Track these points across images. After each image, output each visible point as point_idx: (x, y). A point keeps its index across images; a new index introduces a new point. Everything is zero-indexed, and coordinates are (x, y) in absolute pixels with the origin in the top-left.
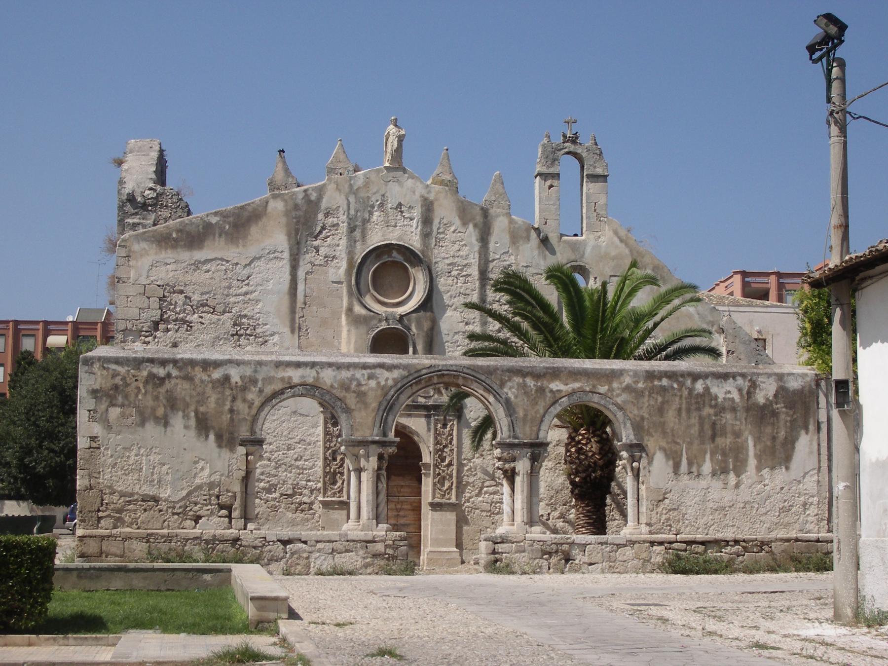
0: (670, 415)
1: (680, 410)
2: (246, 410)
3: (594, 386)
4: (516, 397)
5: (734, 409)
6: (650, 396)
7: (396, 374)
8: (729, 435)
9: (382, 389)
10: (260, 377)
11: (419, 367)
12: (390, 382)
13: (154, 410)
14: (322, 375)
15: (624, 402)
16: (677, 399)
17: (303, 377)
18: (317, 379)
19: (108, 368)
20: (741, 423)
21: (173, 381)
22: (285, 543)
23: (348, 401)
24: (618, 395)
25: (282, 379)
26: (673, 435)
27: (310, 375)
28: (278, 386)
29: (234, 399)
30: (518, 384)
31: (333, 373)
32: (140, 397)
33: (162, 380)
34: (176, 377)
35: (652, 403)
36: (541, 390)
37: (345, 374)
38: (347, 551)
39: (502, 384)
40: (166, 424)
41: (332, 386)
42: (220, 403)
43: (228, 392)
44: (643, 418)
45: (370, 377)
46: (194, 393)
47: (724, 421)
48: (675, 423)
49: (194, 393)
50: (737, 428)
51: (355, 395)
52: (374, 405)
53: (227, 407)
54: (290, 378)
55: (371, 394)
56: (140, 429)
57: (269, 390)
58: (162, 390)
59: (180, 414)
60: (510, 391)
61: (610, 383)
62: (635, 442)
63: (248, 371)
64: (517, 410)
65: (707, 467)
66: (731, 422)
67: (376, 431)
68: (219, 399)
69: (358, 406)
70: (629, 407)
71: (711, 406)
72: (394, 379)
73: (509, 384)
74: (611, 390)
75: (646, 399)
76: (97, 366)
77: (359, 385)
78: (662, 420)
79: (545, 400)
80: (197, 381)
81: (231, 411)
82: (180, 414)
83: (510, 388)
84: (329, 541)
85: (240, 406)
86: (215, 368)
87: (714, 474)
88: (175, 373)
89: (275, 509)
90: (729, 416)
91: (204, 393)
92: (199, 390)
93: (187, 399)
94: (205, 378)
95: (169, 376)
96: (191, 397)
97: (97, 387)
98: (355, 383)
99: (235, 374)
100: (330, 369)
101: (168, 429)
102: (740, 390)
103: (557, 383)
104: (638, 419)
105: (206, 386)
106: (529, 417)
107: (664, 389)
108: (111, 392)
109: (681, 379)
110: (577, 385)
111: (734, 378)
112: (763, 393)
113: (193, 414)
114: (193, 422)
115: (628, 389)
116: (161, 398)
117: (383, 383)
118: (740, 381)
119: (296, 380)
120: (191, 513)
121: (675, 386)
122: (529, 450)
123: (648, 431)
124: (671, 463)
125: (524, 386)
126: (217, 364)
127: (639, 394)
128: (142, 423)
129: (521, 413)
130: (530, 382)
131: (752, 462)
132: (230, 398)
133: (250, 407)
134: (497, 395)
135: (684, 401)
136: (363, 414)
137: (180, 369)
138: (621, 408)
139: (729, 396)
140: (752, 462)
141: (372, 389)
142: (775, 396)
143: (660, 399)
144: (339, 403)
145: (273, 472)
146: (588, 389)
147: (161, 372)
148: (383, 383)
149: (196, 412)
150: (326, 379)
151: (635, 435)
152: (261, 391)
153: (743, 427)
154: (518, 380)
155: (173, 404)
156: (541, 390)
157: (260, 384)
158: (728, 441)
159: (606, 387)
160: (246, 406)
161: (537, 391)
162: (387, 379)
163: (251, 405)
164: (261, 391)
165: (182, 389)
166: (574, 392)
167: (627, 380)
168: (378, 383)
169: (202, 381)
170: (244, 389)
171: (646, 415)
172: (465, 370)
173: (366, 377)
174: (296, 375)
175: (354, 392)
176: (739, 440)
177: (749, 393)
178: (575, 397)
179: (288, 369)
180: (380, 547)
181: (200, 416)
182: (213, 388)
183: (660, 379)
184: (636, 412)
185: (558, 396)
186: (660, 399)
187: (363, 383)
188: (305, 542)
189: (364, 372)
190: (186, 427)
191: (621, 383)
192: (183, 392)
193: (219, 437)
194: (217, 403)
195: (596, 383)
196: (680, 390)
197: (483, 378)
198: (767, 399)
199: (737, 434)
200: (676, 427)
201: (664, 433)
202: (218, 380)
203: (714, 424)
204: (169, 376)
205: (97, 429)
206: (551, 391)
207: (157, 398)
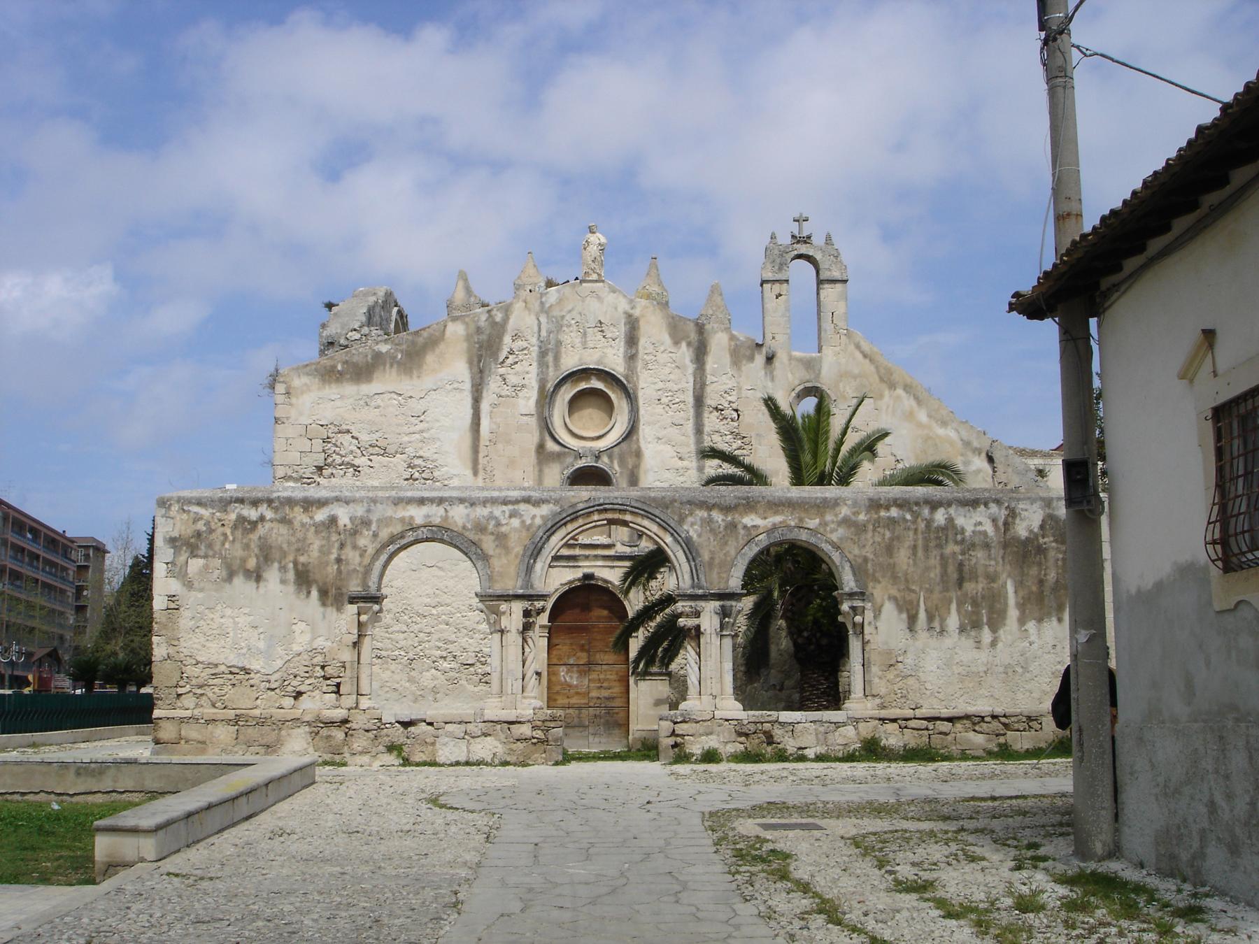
0: (902, 557)
1: (915, 547)
2: (357, 559)
3: (801, 520)
4: (699, 536)
5: (987, 546)
6: (874, 530)
7: (545, 510)
8: (980, 579)
9: (528, 530)
10: (374, 517)
11: (574, 501)
12: (538, 521)
13: (244, 560)
14: (451, 514)
15: (841, 539)
16: (911, 533)
17: (428, 516)
18: (446, 518)
19: (189, 511)
20: (997, 563)
21: (268, 525)
22: (406, 724)
23: (485, 546)
24: (832, 531)
25: (402, 520)
26: (907, 581)
27: (436, 513)
28: (397, 529)
29: (342, 546)
30: (702, 519)
31: (466, 511)
32: (227, 545)
33: (254, 524)
34: (271, 521)
35: (878, 539)
36: (732, 526)
37: (481, 512)
38: (486, 735)
39: (682, 520)
40: (259, 578)
41: (464, 527)
42: (324, 552)
43: (334, 537)
44: (866, 560)
45: (513, 515)
46: (293, 540)
47: (974, 561)
48: (908, 565)
49: (293, 540)
50: (991, 569)
51: (492, 537)
52: (519, 550)
53: (333, 556)
54: (412, 518)
55: (514, 537)
56: (227, 585)
57: (385, 534)
58: (254, 537)
59: (276, 565)
60: (692, 529)
61: (822, 515)
62: (856, 590)
63: (360, 511)
64: (701, 551)
65: (953, 621)
66: (983, 562)
67: (519, 583)
68: (322, 546)
69: (498, 551)
70: (848, 546)
71: (956, 542)
72: (542, 517)
73: (690, 519)
74: (824, 524)
75: (870, 534)
76: (175, 507)
77: (498, 524)
78: (891, 561)
79: (737, 538)
80: (297, 524)
81: (339, 560)
82: (276, 565)
83: (692, 524)
84: (460, 723)
85: (351, 555)
86: (318, 508)
87: (962, 630)
88: (269, 514)
89: (454, 682)
90: (980, 554)
91: (305, 539)
92: (299, 535)
93: (285, 546)
94: (306, 520)
95: (262, 518)
96: (289, 543)
97: (175, 534)
98: (493, 523)
99: (344, 516)
100: (461, 506)
101: (261, 584)
102: (994, 521)
103: (753, 516)
104: (860, 560)
105: (308, 530)
106: (717, 561)
107: (892, 522)
108: (192, 540)
109: (915, 508)
110: (778, 519)
111: (986, 505)
112: (1025, 524)
113: (291, 565)
114: (291, 575)
115: (846, 522)
116: (253, 545)
117: (528, 522)
118: (994, 508)
119: (419, 521)
120: (290, 689)
121: (908, 517)
122: (717, 604)
123: (873, 575)
124: (904, 616)
125: (710, 521)
126: (322, 503)
127: (860, 528)
128: (231, 576)
129: (706, 556)
130: (717, 516)
131: (1013, 613)
132: (337, 545)
133: (361, 556)
134: (674, 533)
135: (920, 536)
136: (504, 561)
137: (276, 510)
138: (837, 547)
139: (979, 528)
140: (1013, 613)
141: (515, 530)
142: (1042, 527)
143: (888, 534)
144: (473, 549)
145: (453, 637)
146: (793, 524)
147: (253, 514)
148: (528, 522)
149: (295, 563)
150: (457, 518)
151: (856, 581)
152: (375, 535)
153: (999, 568)
154: (702, 514)
155: (267, 554)
156: (732, 526)
157: (374, 527)
158: (980, 586)
159: (817, 521)
160: (357, 553)
161: (726, 528)
162: (534, 517)
163: (363, 553)
164: (375, 535)
165: (278, 534)
166: (775, 528)
167: (844, 511)
168: (523, 522)
169: (303, 525)
170: (355, 533)
171: (871, 556)
172: (634, 504)
173: (507, 514)
174: (418, 514)
175: (492, 534)
176: (995, 585)
177: (1006, 524)
178: (776, 534)
179: (409, 507)
180: (526, 730)
181: (300, 567)
182: (316, 532)
183: (887, 508)
184: (856, 551)
185: (754, 533)
186: (888, 534)
187: (504, 522)
188: (431, 724)
189: (504, 508)
190: (283, 582)
191: (836, 515)
192: (280, 539)
193: (324, 593)
194: (320, 551)
195: (803, 515)
196: (914, 522)
197: (657, 512)
198: (1031, 531)
199: (992, 578)
200: (911, 569)
201: (895, 578)
202: (323, 523)
203: (961, 565)
204: (262, 518)
205: (175, 586)
206: (745, 527)
207: (247, 547)
